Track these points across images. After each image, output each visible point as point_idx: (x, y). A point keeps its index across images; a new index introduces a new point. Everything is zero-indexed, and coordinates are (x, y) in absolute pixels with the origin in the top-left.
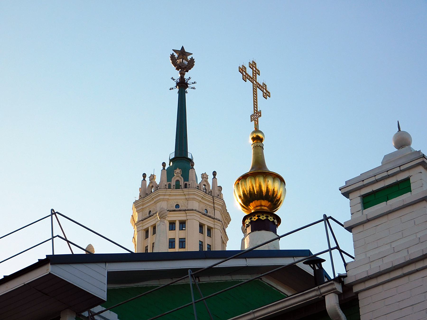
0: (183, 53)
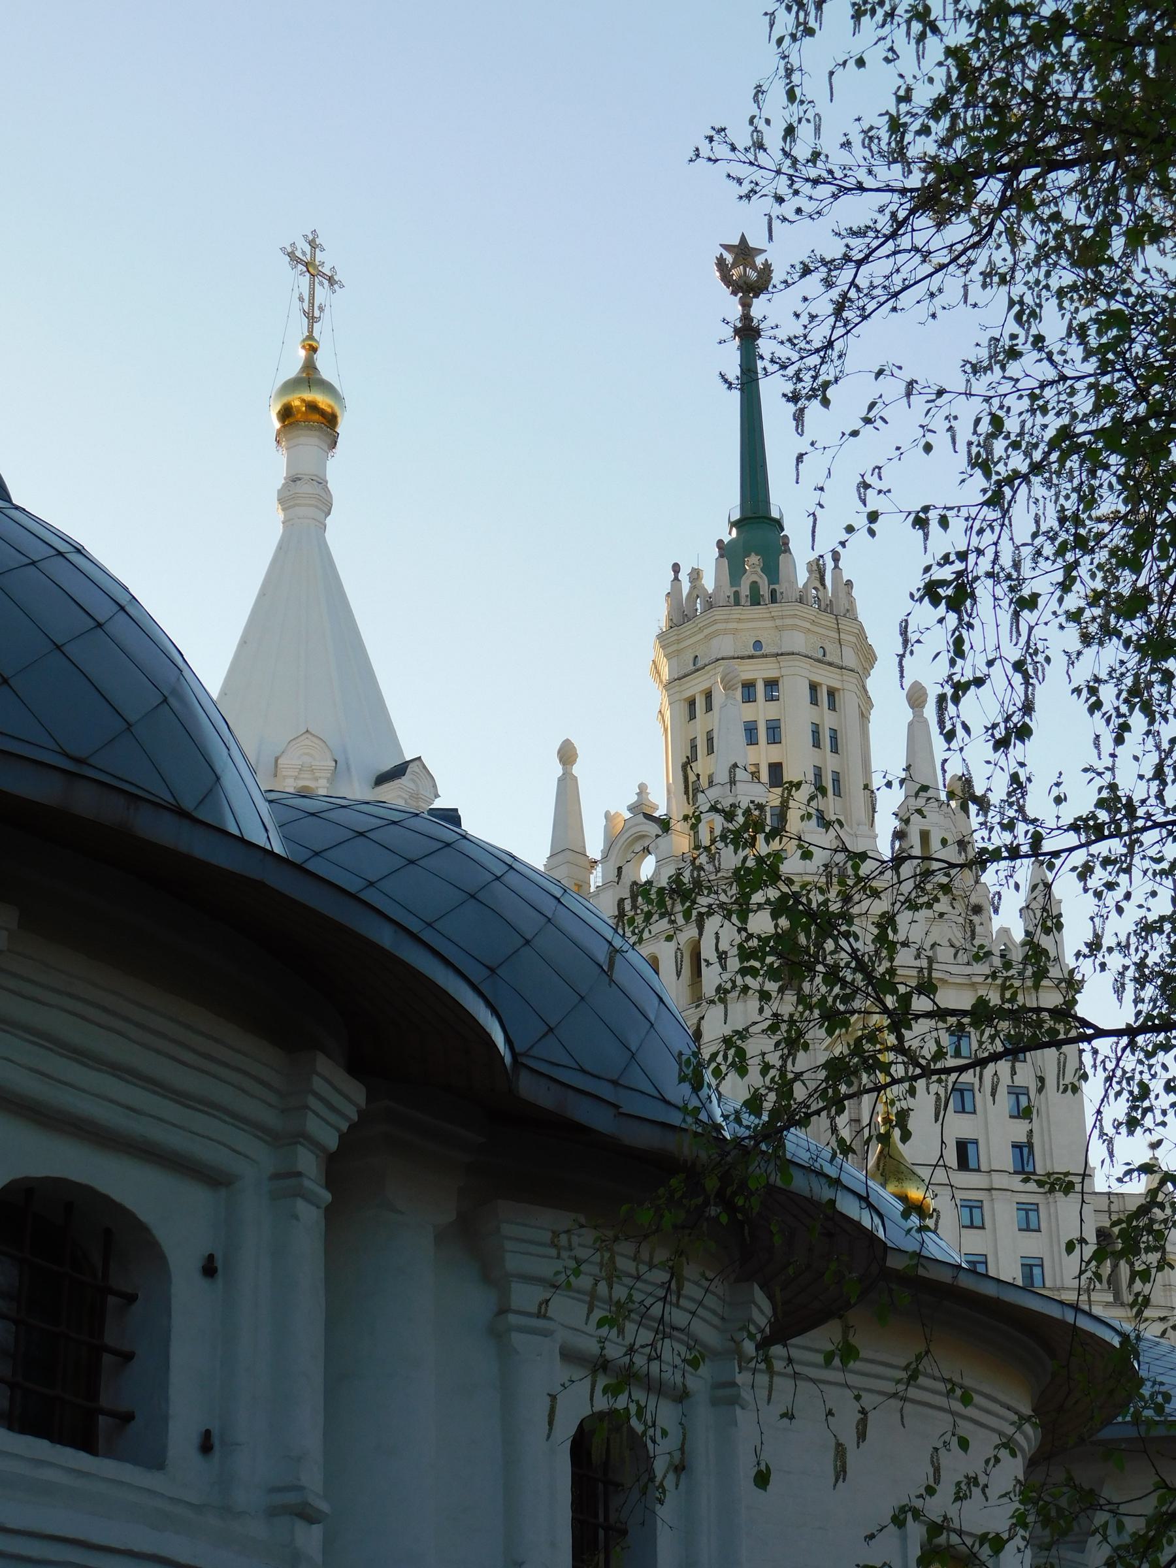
0: (744, 251)
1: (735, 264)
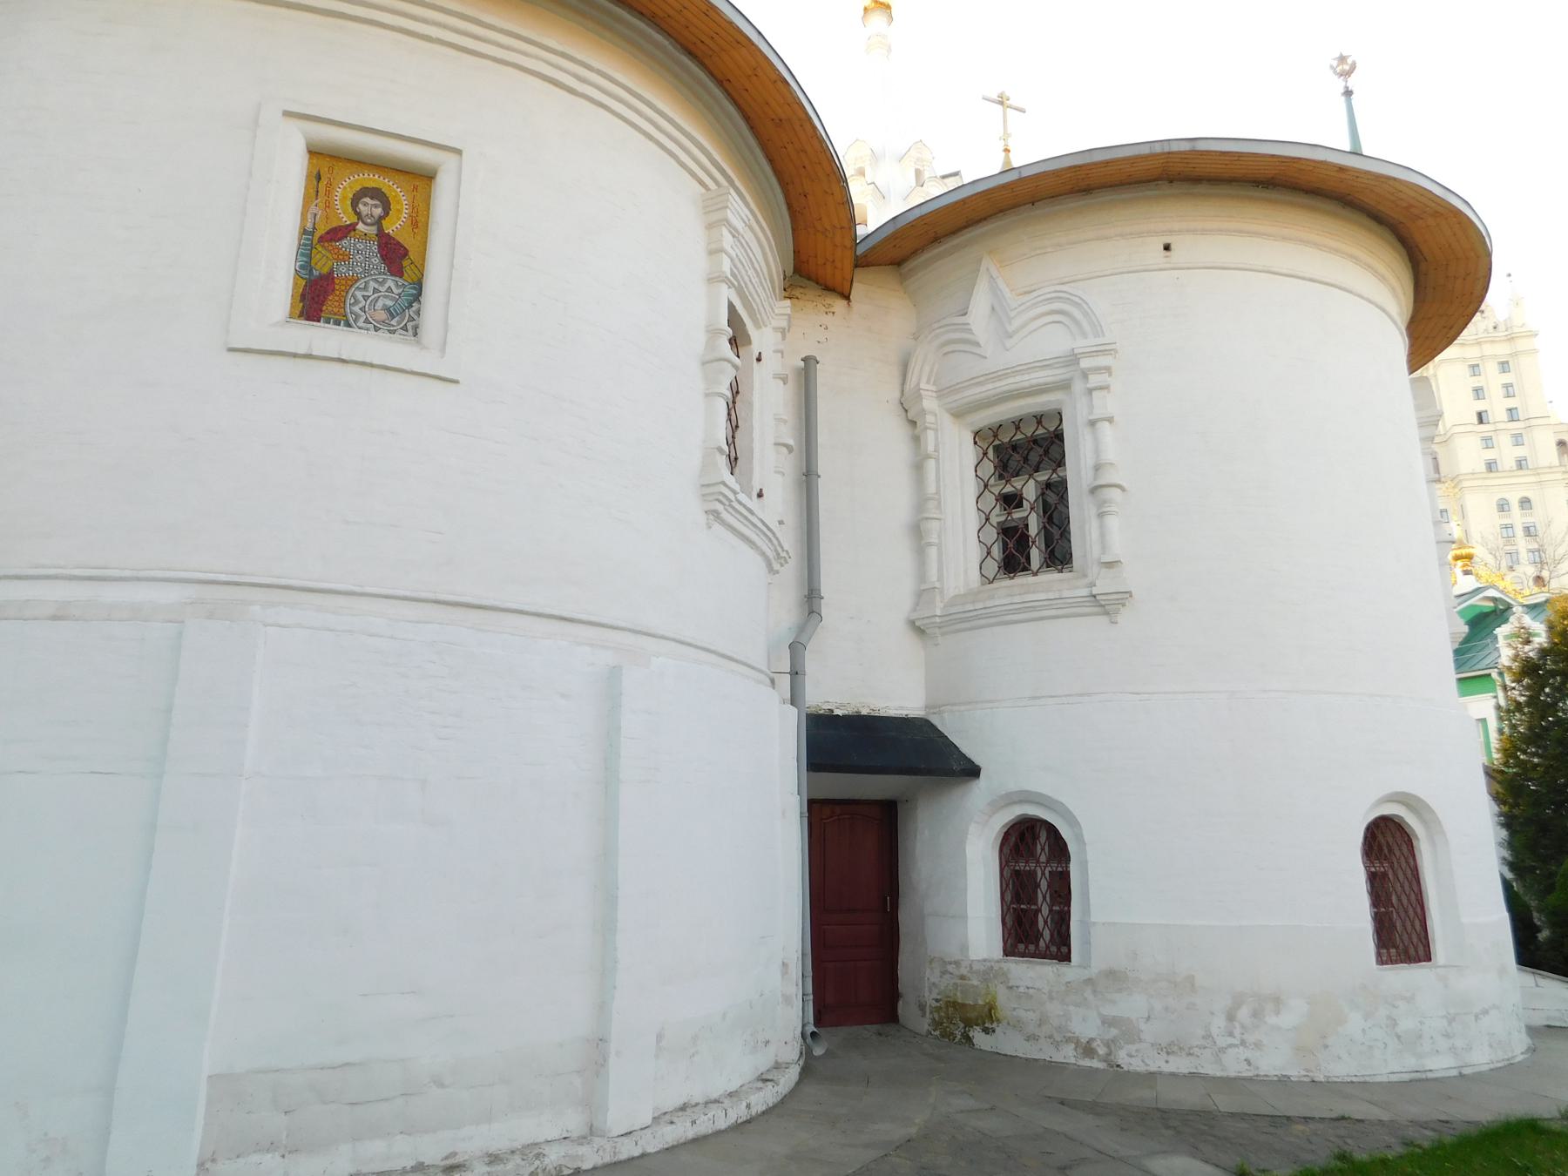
1: (1338, 66)
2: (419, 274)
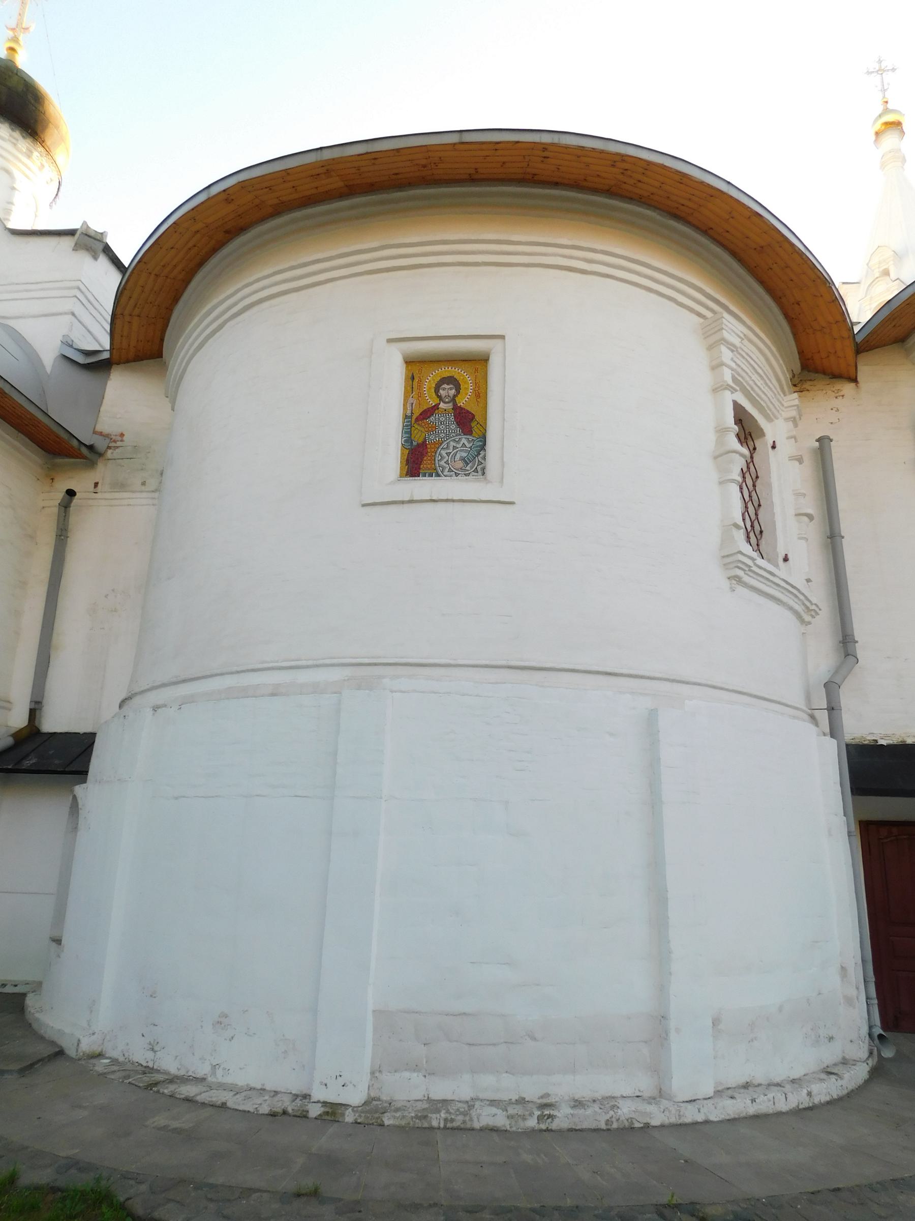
2: (484, 431)
